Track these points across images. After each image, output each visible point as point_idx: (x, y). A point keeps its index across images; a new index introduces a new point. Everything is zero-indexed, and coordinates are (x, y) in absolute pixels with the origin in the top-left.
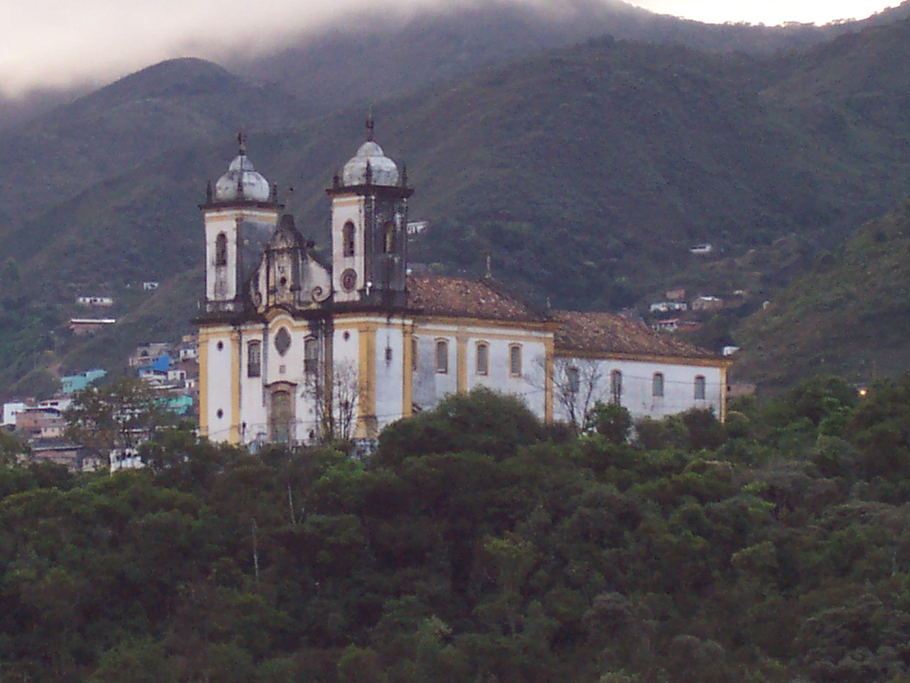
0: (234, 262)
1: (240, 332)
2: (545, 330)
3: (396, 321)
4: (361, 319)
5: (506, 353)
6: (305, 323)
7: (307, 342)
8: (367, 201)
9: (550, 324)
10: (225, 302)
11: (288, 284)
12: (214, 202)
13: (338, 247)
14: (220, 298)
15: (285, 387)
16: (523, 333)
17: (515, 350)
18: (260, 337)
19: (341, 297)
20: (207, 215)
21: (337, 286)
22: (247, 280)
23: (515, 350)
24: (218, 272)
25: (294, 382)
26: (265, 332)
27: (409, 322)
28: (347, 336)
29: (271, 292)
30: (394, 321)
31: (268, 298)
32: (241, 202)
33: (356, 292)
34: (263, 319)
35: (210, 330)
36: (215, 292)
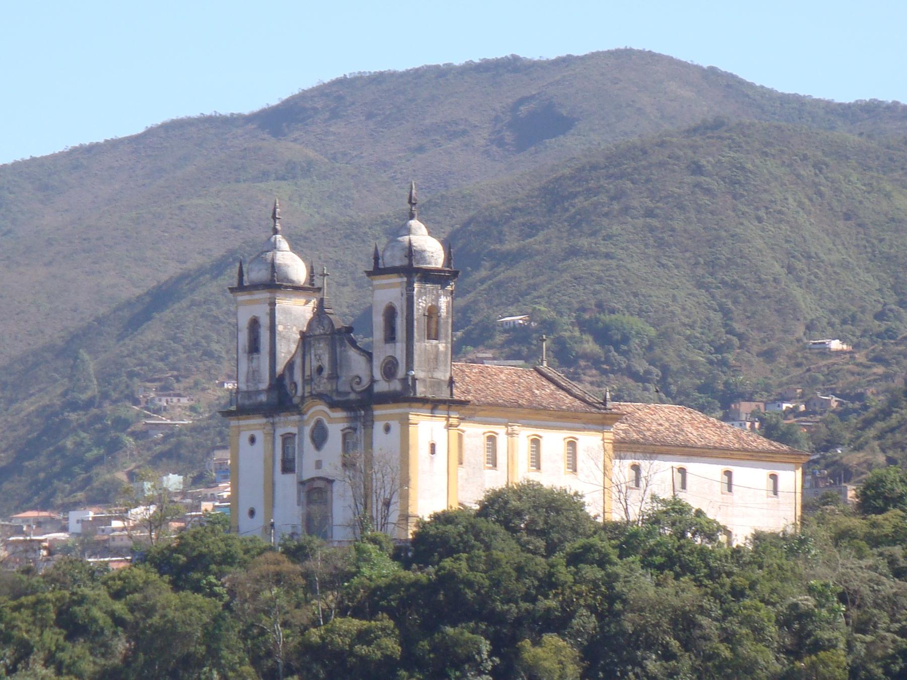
1: (273, 424)
6: (340, 414)
7: (345, 437)
10: (258, 392)
11: (326, 373)
13: (379, 333)
14: (252, 388)
15: (320, 484)
18: (294, 430)
19: (382, 386)
21: (378, 375)
24: (250, 360)
25: (330, 478)
26: (301, 425)
28: (387, 429)
29: (307, 381)
31: (304, 388)
33: (397, 381)
34: (297, 409)
35: (242, 423)
36: (247, 381)
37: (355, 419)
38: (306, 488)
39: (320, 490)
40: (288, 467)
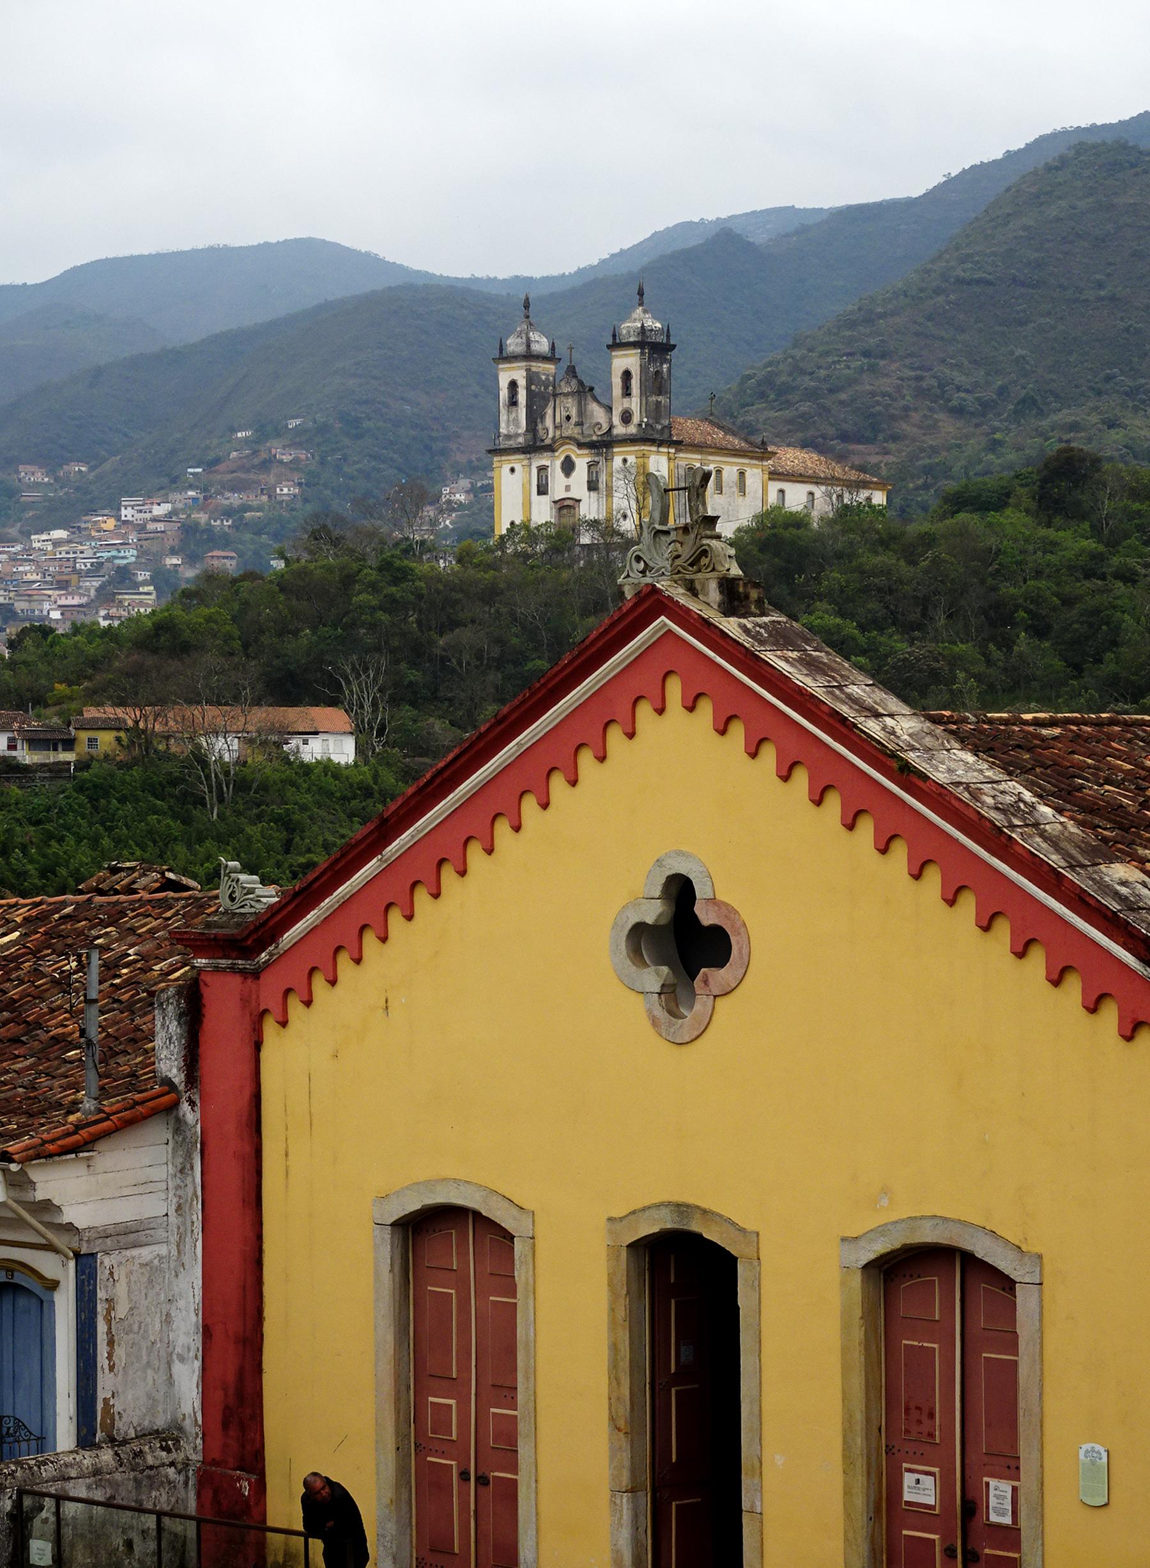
0: (524, 403)
2: (762, 459)
3: (664, 450)
4: (636, 448)
5: (735, 476)
6: (586, 451)
7: (589, 467)
8: (642, 354)
9: (767, 455)
10: (519, 435)
11: (574, 419)
12: (505, 355)
13: (617, 390)
16: (746, 461)
17: (742, 474)
18: (547, 463)
19: (620, 430)
20: (501, 366)
21: (616, 420)
22: (534, 417)
23: (742, 474)
27: (672, 451)
30: (661, 449)
32: (529, 356)
34: (550, 448)
35: (503, 458)
36: (508, 426)
37: (598, 454)
38: (558, 506)
39: (568, 507)
40: (542, 490)
